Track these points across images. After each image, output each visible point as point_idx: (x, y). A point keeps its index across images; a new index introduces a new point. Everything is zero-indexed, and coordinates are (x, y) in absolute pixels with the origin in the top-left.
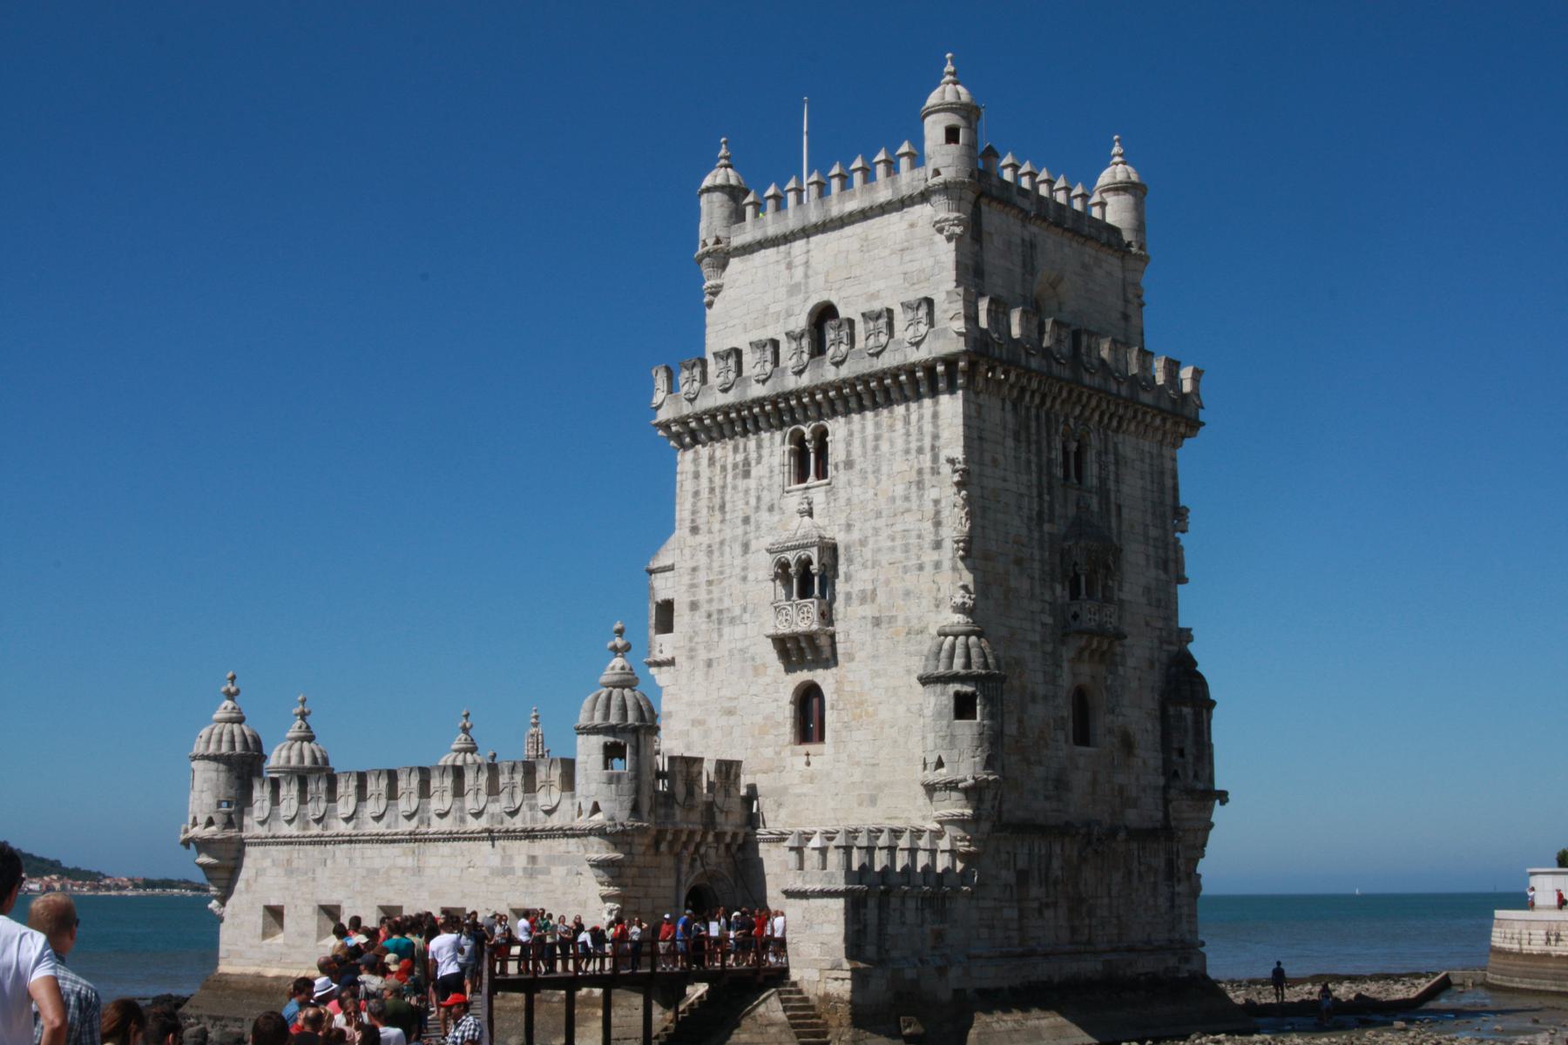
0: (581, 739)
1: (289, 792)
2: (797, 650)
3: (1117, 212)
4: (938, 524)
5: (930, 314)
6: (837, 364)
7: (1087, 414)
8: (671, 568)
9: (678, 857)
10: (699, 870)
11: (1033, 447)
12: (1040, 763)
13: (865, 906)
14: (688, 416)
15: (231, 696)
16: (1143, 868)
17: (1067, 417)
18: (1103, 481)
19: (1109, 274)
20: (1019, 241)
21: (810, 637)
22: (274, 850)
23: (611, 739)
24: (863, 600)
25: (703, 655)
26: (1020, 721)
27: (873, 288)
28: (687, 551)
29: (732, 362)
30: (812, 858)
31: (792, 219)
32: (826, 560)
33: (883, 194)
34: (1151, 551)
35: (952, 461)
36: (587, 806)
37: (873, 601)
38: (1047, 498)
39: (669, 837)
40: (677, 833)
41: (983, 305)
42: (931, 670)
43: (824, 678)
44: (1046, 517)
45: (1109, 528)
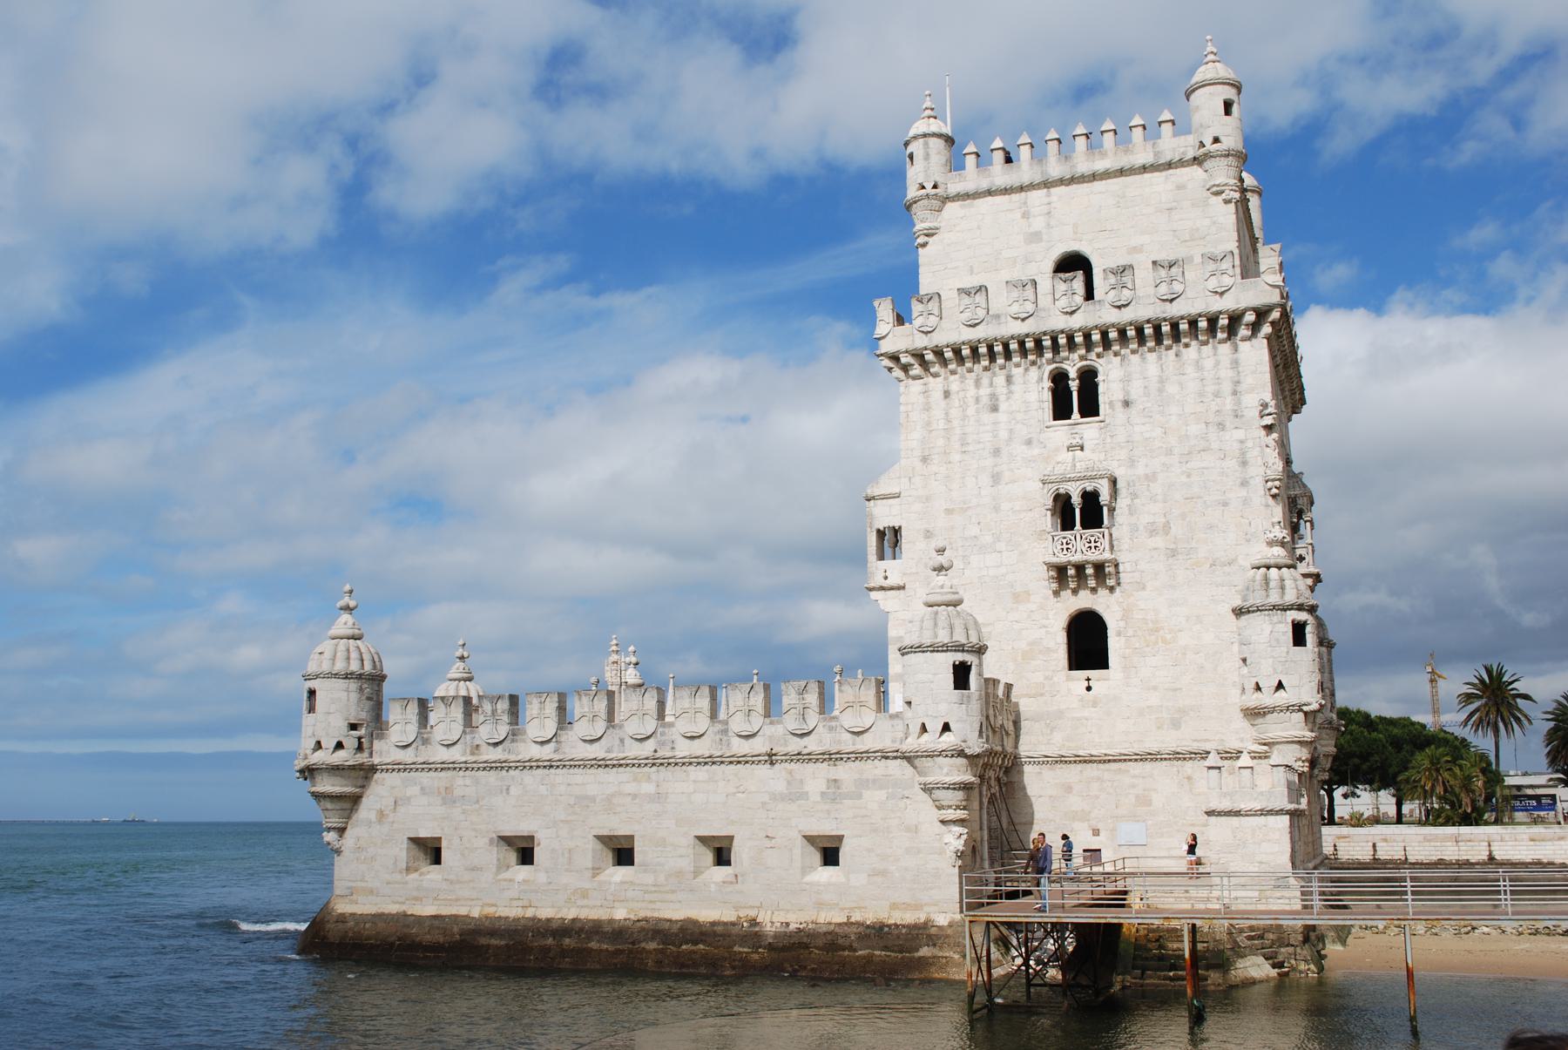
21: (1099, 567)
22: (425, 778)
23: (960, 657)
24: (1153, 532)
33: (1143, 157)
42: (1257, 599)
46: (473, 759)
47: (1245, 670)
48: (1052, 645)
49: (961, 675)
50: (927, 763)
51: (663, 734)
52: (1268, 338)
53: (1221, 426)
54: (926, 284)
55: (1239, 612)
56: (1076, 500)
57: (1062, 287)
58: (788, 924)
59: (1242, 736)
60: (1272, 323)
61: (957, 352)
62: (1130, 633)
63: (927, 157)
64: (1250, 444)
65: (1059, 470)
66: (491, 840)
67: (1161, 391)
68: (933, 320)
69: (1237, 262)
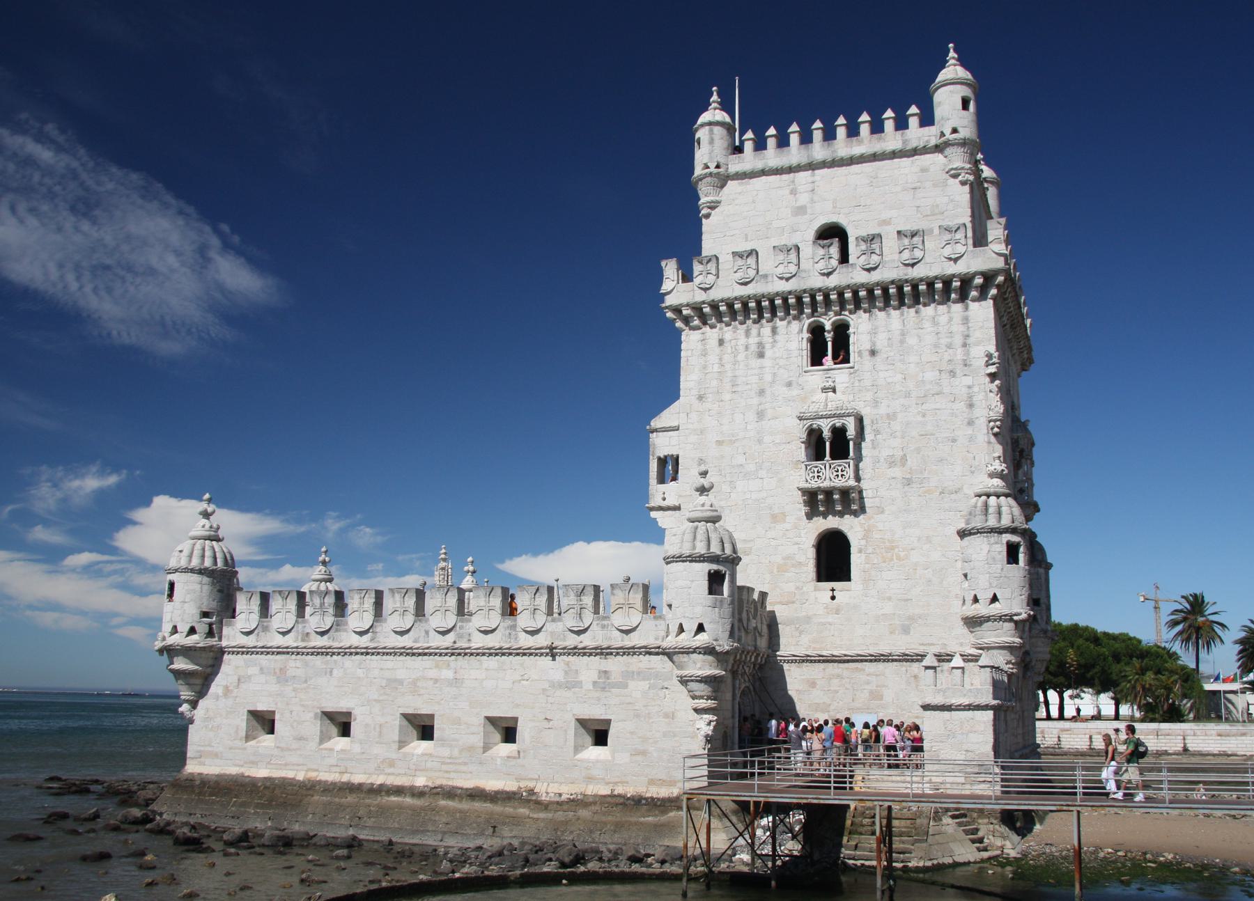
2: (816, 501)
8: (677, 429)
14: (704, 302)
21: (845, 493)
23: (714, 567)
24: (892, 464)
27: (886, 215)
28: (694, 416)
37: (903, 465)
42: (977, 523)
43: (849, 525)
46: (303, 644)
47: (966, 584)
48: (802, 559)
49: (715, 581)
50: (684, 658)
51: (461, 628)
52: (994, 299)
53: (952, 373)
54: (708, 248)
55: (963, 534)
56: (827, 434)
57: (821, 252)
58: (560, 795)
59: (961, 641)
60: (998, 286)
61: (730, 305)
62: (870, 550)
63: (711, 142)
64: (976, 389)
65: (813, 409)
66: (316, 714)
67: (902, 342)
68: (711, 279)
69: (970, 234)
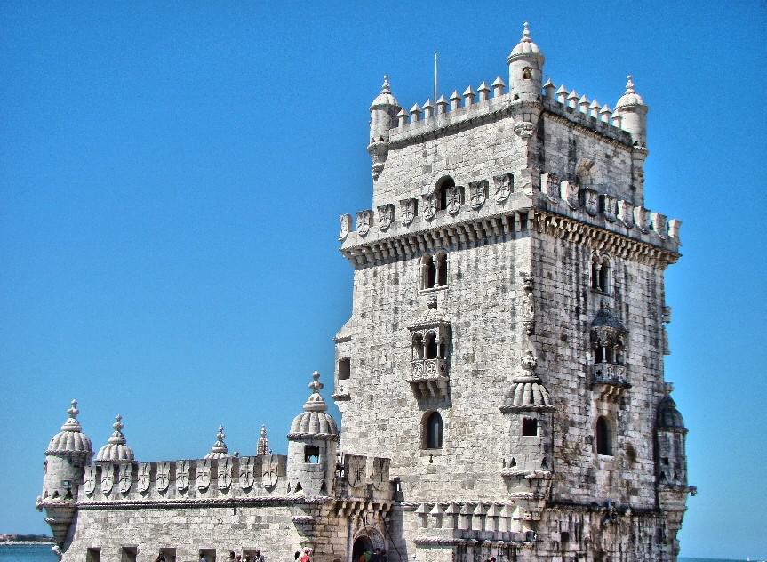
0: (291, 443)
1: (107, 475)
3: (628, 124)
4: (514, 314)
5: (511, 184)
6: (453, 215)
7: (608, 246)
8: (348, 339)
9: (350, 519)
10: (362, 528)
11: (574, 268)
12: (576, 465)
13: (466, 552)
15: (73, 415)
16: (642, 534)
17: (595, 249)
18: (617, 289)
19: (623, 162)
20: (567, 140)
21: (434, 382)
23: (309, 444)
24: (467, 360)
25: (368, 392)
26: (564, 437)
29: (388, 213)
30: (433, 521)
31: (426, 127)
32: (445, 335)
33: (483, 110)
34: (647, 333)
35: (522, 274)
36: (294, 485)
38: (582, 299)
39: (344, 506)
40: (349, 504)
41: (545, 178)
44: (582, 311)
45: (621, 319)
48: (414, 432)
49: (310, 451)
